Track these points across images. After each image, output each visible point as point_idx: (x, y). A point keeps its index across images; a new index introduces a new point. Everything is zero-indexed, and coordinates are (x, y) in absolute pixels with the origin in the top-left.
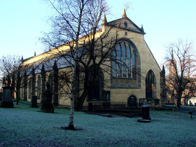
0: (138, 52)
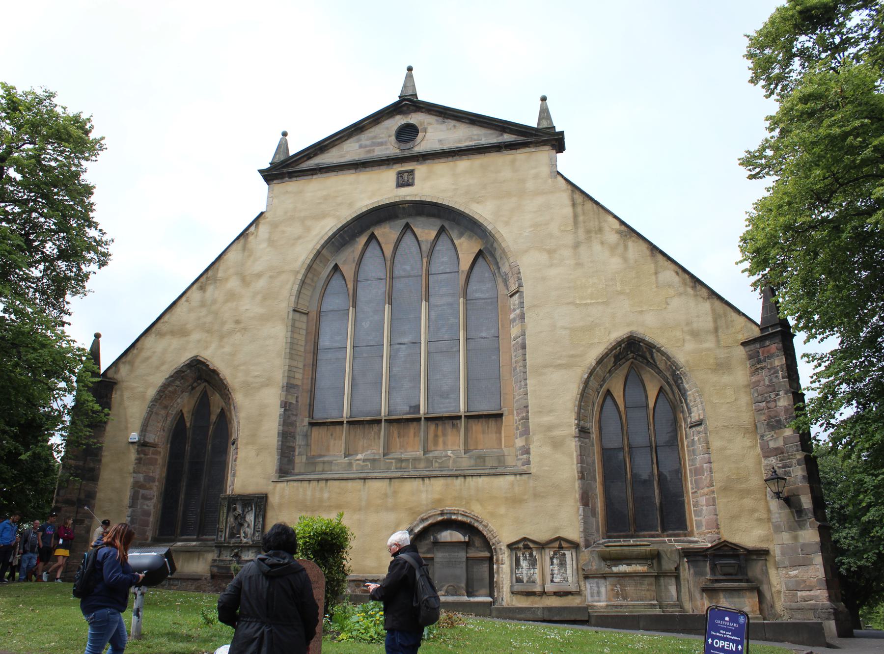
0: (503, 251)
